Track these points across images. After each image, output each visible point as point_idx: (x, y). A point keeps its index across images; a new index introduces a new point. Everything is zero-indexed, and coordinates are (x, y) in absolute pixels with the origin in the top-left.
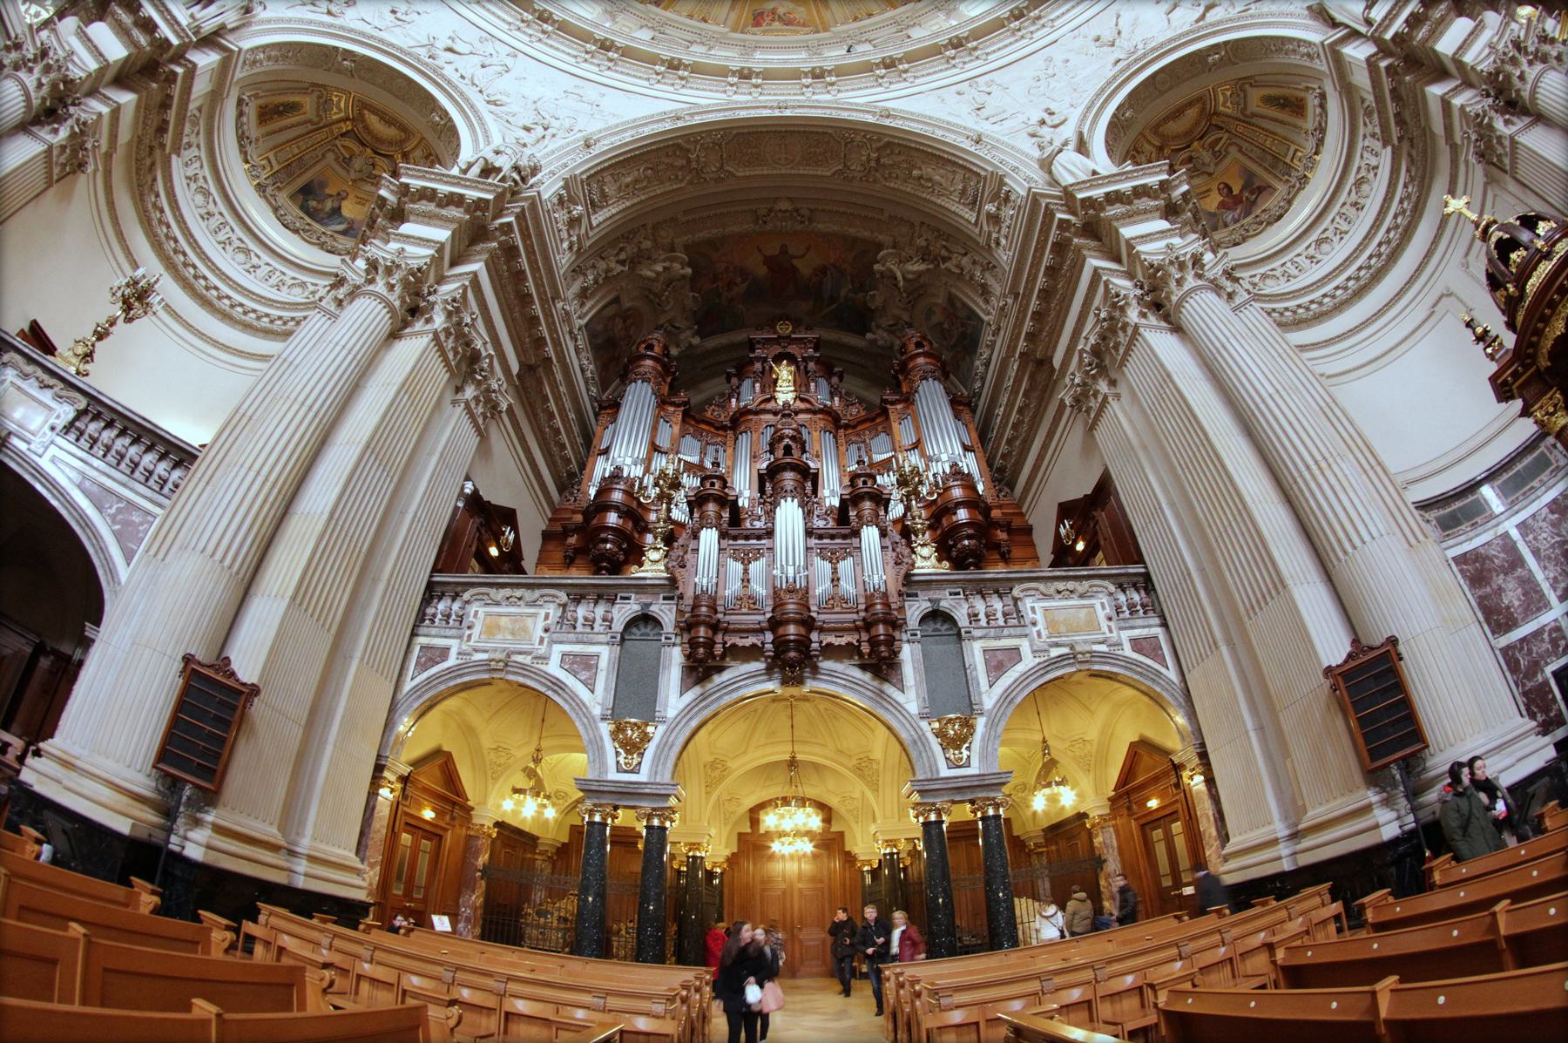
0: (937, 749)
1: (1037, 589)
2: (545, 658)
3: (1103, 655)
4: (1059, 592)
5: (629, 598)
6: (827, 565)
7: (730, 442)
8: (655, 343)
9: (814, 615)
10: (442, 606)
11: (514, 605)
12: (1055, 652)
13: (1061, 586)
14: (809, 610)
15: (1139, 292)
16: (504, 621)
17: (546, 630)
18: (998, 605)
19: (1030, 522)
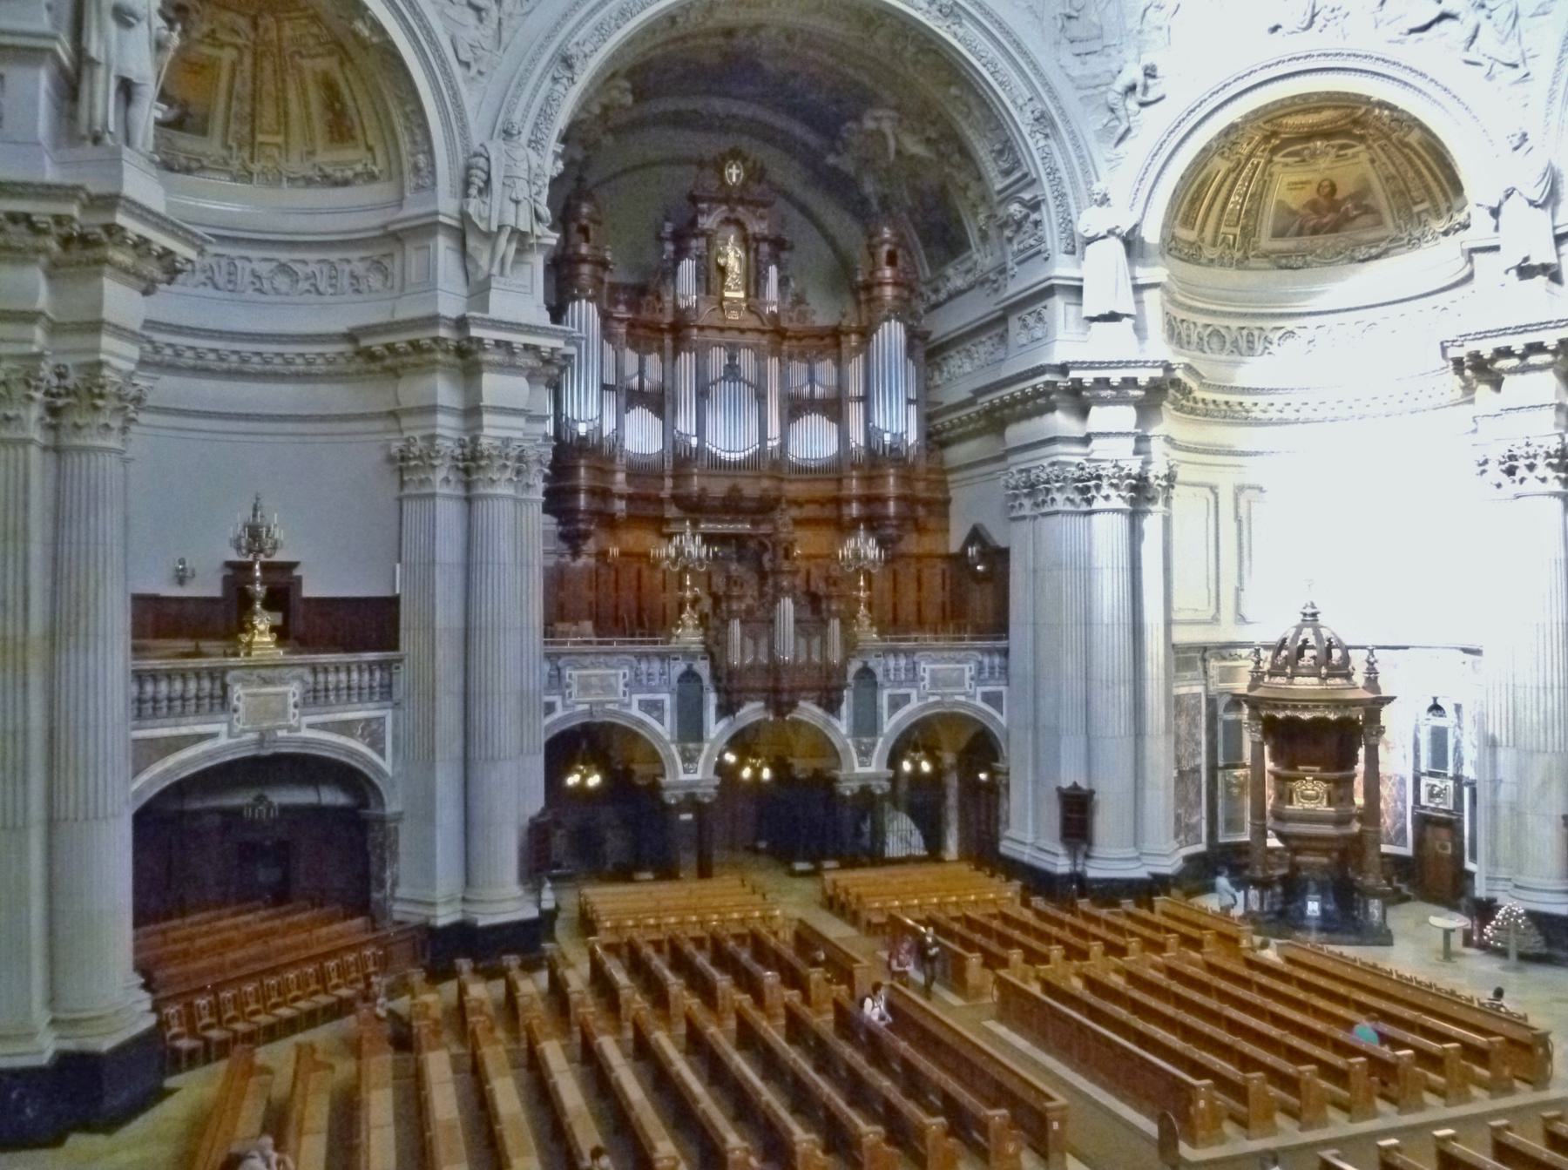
0: (855, 755)
2: (629, 705)
3: (962, 704)
7: (669, 353)
12: (932, 699)
13: (946, 654)
17: (626, 685)
18: (902, 662)
19: (952, 493)
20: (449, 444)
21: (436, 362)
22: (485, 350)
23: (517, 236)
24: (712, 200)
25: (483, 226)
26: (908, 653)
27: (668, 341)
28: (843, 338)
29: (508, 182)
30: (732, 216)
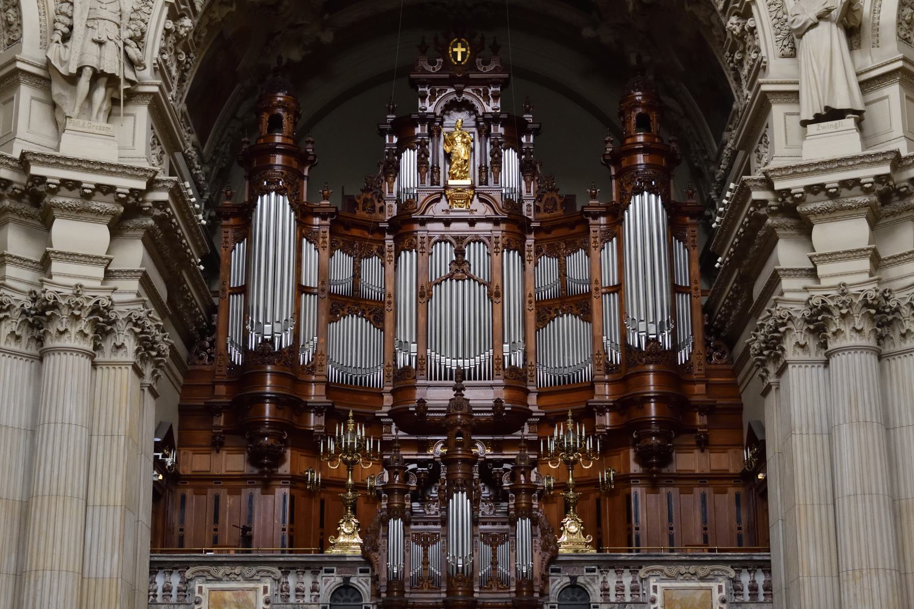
1: (662, 571)
4: (682, 575)
5: (332, 571)
6: (489, 548)
7: (390, 255)
8: (280, 111)
9: (476, 595)
10: (160, 581)
11: (235, 580)
13: (683, 569)
14: (474, 592)
15: (807, 313)
16: (228, 595)
17: (267, 602)
18: (627, 580)
19: (743, 400)
20: (23, 298)
21: (6, 210)
22: (54, 192)
23: (104, 80)
24: (431, 83)
25: (62, 70)
26: (634, 566)
27: (389, 241)
28: (591, 221)
29: (90, 24)
30: (459, 100)
